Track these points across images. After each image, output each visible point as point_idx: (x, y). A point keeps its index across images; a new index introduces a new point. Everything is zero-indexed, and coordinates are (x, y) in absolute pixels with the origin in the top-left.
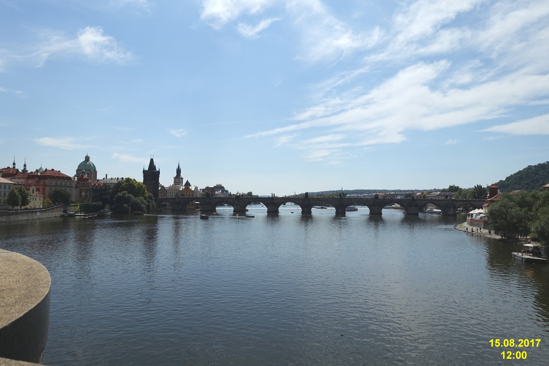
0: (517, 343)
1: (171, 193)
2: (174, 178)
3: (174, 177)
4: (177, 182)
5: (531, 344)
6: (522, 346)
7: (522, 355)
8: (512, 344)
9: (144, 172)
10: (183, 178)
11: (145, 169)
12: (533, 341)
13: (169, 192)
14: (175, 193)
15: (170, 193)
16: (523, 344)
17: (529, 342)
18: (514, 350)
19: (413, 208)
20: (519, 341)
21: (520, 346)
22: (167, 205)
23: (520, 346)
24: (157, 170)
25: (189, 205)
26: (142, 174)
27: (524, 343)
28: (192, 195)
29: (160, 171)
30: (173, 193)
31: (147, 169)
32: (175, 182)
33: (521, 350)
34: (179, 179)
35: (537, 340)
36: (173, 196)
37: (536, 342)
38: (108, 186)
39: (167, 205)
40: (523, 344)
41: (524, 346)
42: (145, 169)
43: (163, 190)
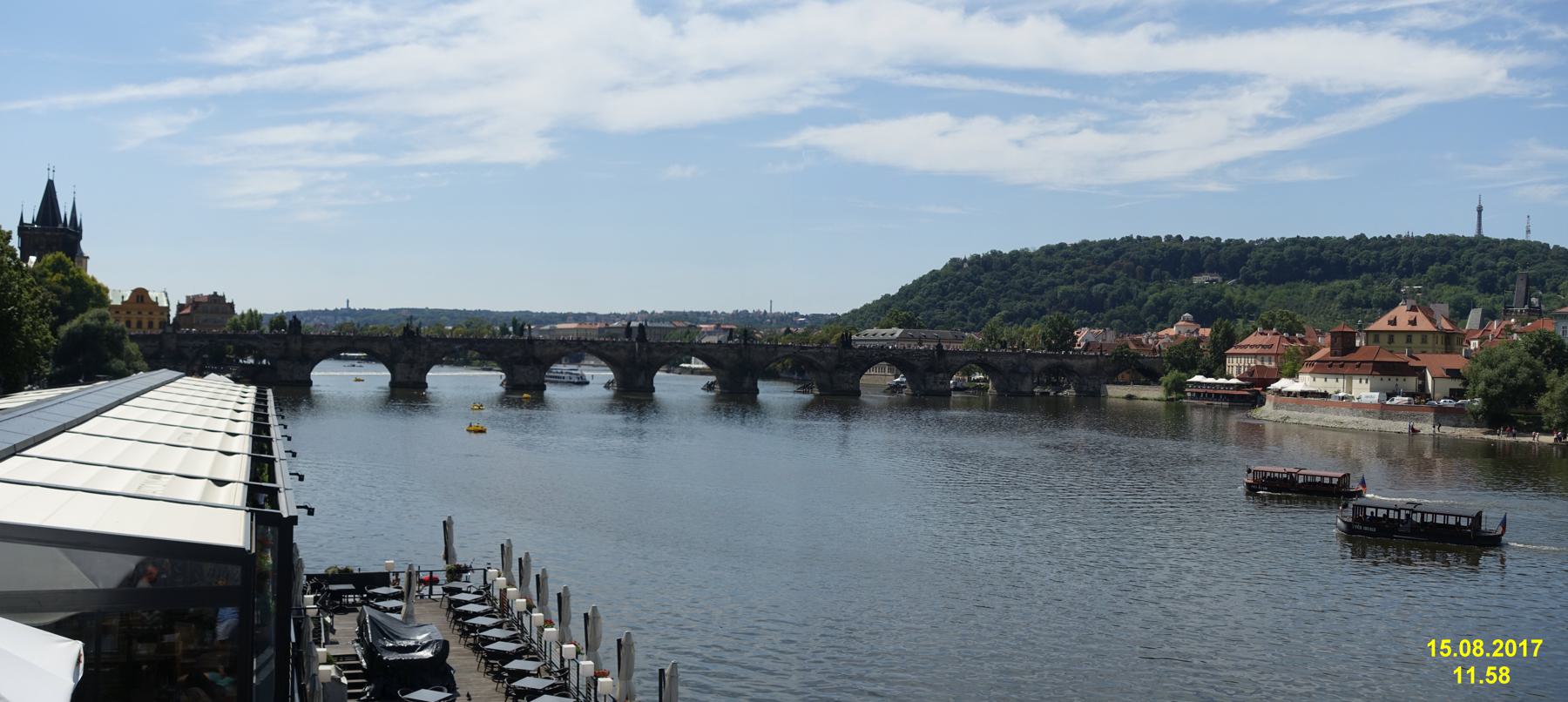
0: (1489, 648)
5: (1520, 649)
6: (1502, 655)
7: (1504, 675)
8: (1478, 651)
12: (1524, 643)
16: (1503, 651)
17: (1518, 645)
18: (1481, 664)
19: (941, 375)
20: (1495, 643)
21: (1496, 654)
23: (1496, 654)
27: (1507, 647)
33: (1499, 662)
35: (1533, 641)
37: (1531, 647)
40: (1503, 651)
41: (1505, 654)
42: (25, 221)
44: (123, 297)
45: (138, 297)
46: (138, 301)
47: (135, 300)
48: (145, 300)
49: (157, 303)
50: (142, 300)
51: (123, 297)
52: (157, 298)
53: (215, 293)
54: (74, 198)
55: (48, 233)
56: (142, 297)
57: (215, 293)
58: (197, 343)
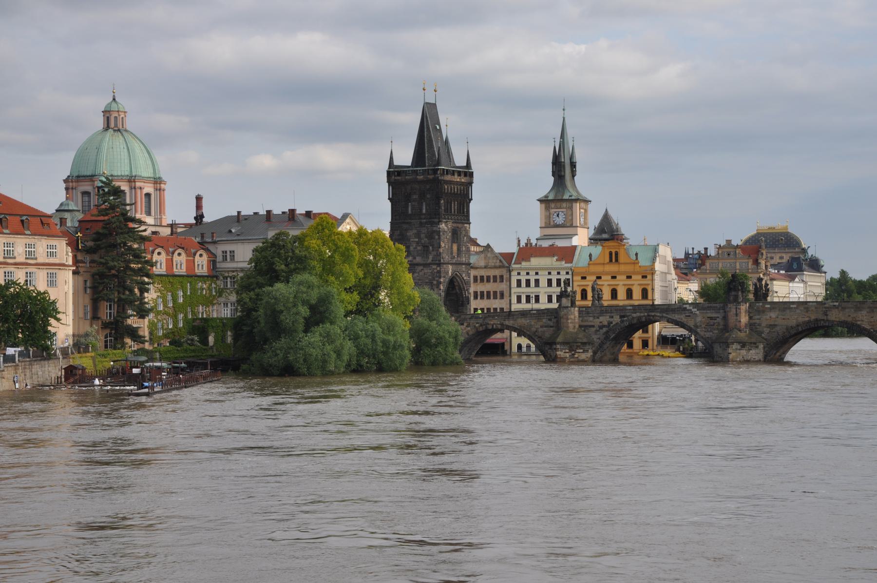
1: (532, 283)
2: (540, 201)
3: (542, 194)
4: (557, 226)
9: (395, 175)
10: (587, 201)
11: (396, 163)
13: (519, 282)
14: (550, 282)
15: (528, 283)
22: (515, 349)
24: (459, 160)
25: (630, 345)
26: (384, 189)
28: (645, 294)
29: (474, 168)
30: (543, 282)
31: (405, 157)
32: (548, 224)
34: (571, 208)
36: (543, 299)
38: (225, 259)
39: (515, 349)
42: (396, 163)
43: (486, 267)
44: (590, 255)
45: (611, 254)
46: (611, 260)
47: (607, 260)
48: (621, 259)
49: (636, 262)
50: (617, 260)
51: (590, 255)
52: (637, 254)
53: (729, 242)
54: (564, 118)
55: (420, 177)
56: (617, 253)
57: (729, 242)
58: (604, 319)
